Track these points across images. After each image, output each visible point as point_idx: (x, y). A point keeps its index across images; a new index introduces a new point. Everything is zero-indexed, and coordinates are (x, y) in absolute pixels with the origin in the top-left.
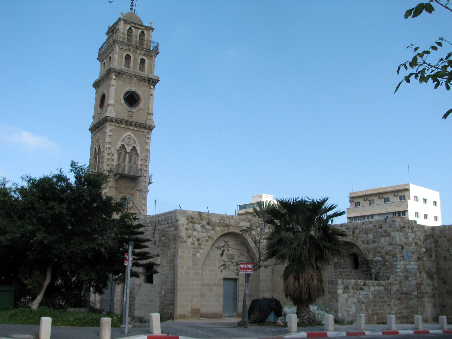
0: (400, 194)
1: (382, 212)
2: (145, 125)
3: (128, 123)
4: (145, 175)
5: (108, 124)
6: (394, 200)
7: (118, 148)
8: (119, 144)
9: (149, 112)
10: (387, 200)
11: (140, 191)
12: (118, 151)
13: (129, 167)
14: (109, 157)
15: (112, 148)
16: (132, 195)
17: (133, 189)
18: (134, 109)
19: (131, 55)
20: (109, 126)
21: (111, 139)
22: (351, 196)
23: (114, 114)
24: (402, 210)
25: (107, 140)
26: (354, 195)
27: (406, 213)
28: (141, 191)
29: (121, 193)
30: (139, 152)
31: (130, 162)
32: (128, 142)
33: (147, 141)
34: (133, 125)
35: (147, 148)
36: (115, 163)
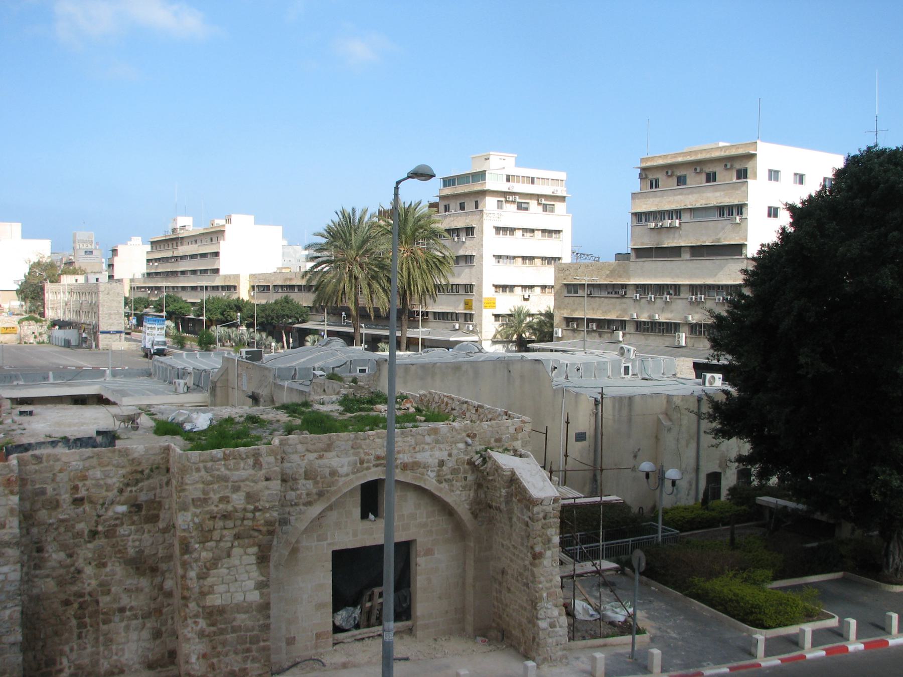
0: (738, 166)
1: (698, 205)
6: (727, 177)
10: (711, 178)
22: (644, 165)
24: (736, 202)
26: (649, 164)
27: (744, 210)
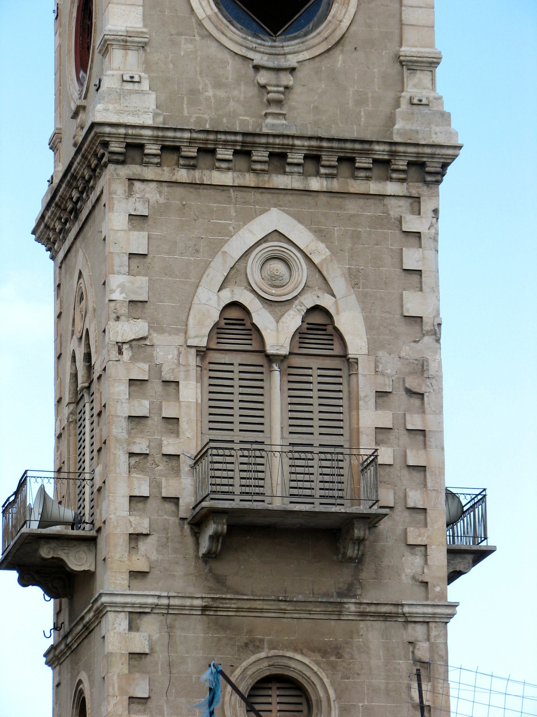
2: (381, 151)
3: (261, 154)
4: (415, 498)
5: (112, 180)
7: (199, 334)
8: (209, 305)
9: (406, 50)
11: (386, 617)
12: (201, 353)
13: (297, 452)
14: (142, 408)
15: (156, 338)
16: (331, 652)
17: (336, 609)
18: (291, 45)
20: (119, 188)
21: (142, 281)
23: (150, 101)
25: (122, 285)
28: (393, 616)
29: (252, 645)
30: (357, 344)
31: (297, 421)
32: (275, 282)
33: (412, 259)
34: (296, 157)
35: (413, 305)
36: (188, 441)
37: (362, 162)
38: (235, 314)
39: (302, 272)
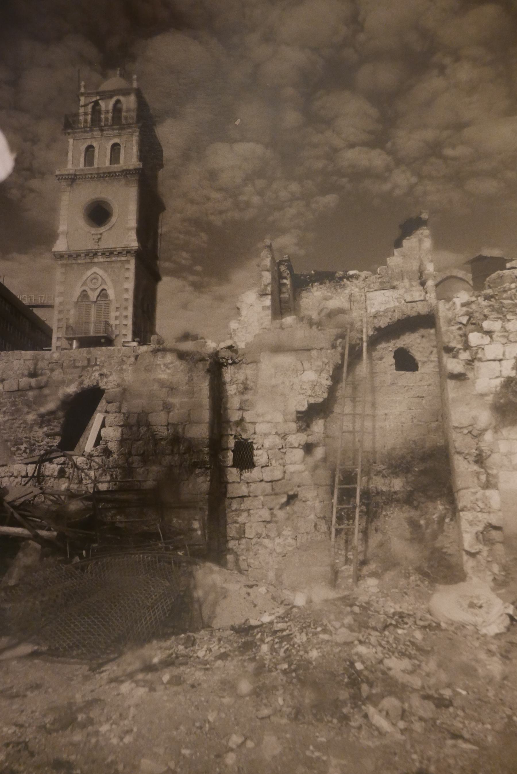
7: (75, 299)
19: (94, 145)
37: (115, 253)
38: (84, 293)
39: (100, 280)
